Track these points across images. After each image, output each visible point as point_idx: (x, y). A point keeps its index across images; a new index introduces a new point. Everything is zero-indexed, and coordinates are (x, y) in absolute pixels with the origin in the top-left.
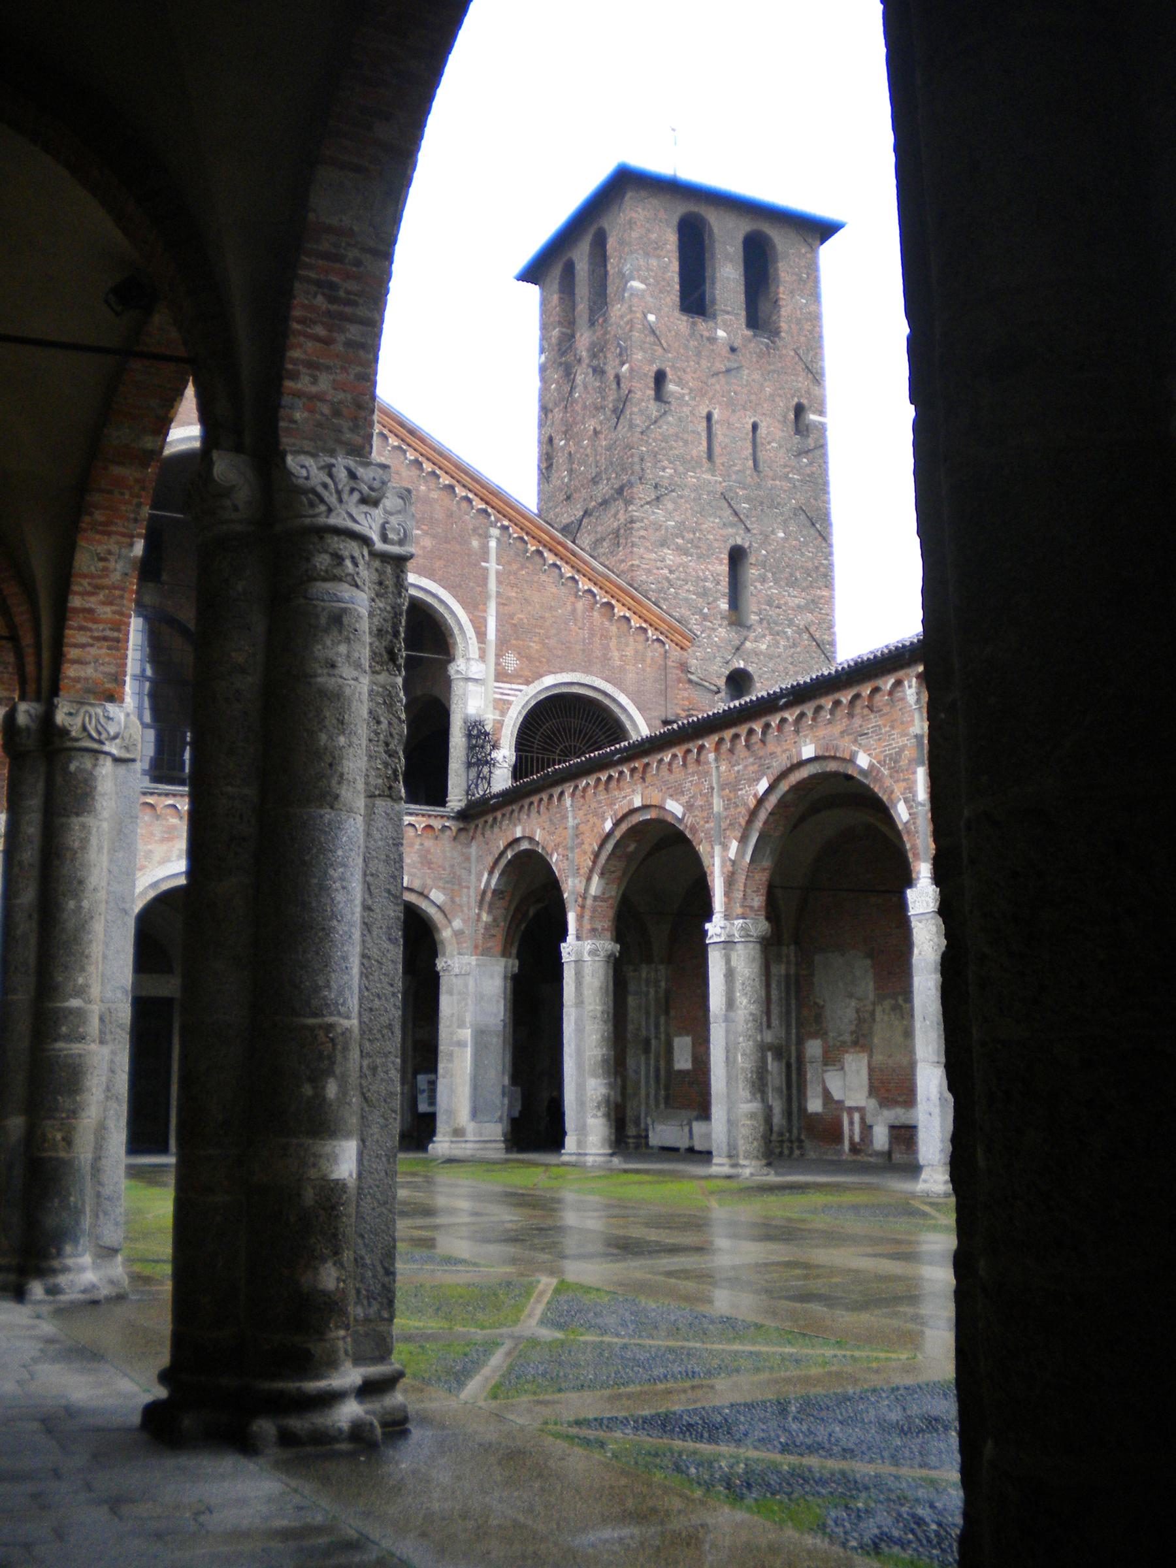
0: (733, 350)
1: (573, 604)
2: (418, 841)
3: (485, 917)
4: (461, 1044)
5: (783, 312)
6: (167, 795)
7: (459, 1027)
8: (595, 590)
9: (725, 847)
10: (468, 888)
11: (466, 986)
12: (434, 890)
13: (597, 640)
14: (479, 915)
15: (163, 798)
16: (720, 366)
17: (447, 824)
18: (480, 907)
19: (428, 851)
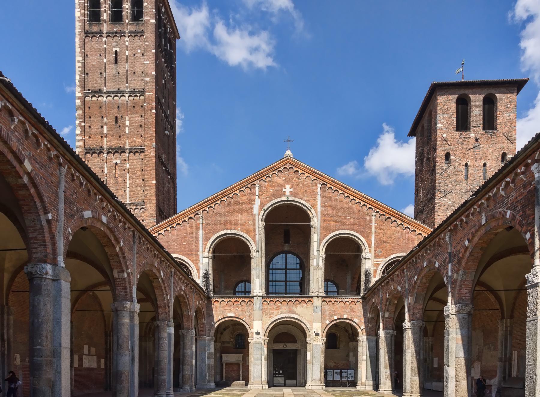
0: (477, 140)
1: (402, 232)
5: (498, 121)
6: (277, 298)
8: (409, 227)
9: (408, 299)
13: (410, 242)
16: (471, 146)
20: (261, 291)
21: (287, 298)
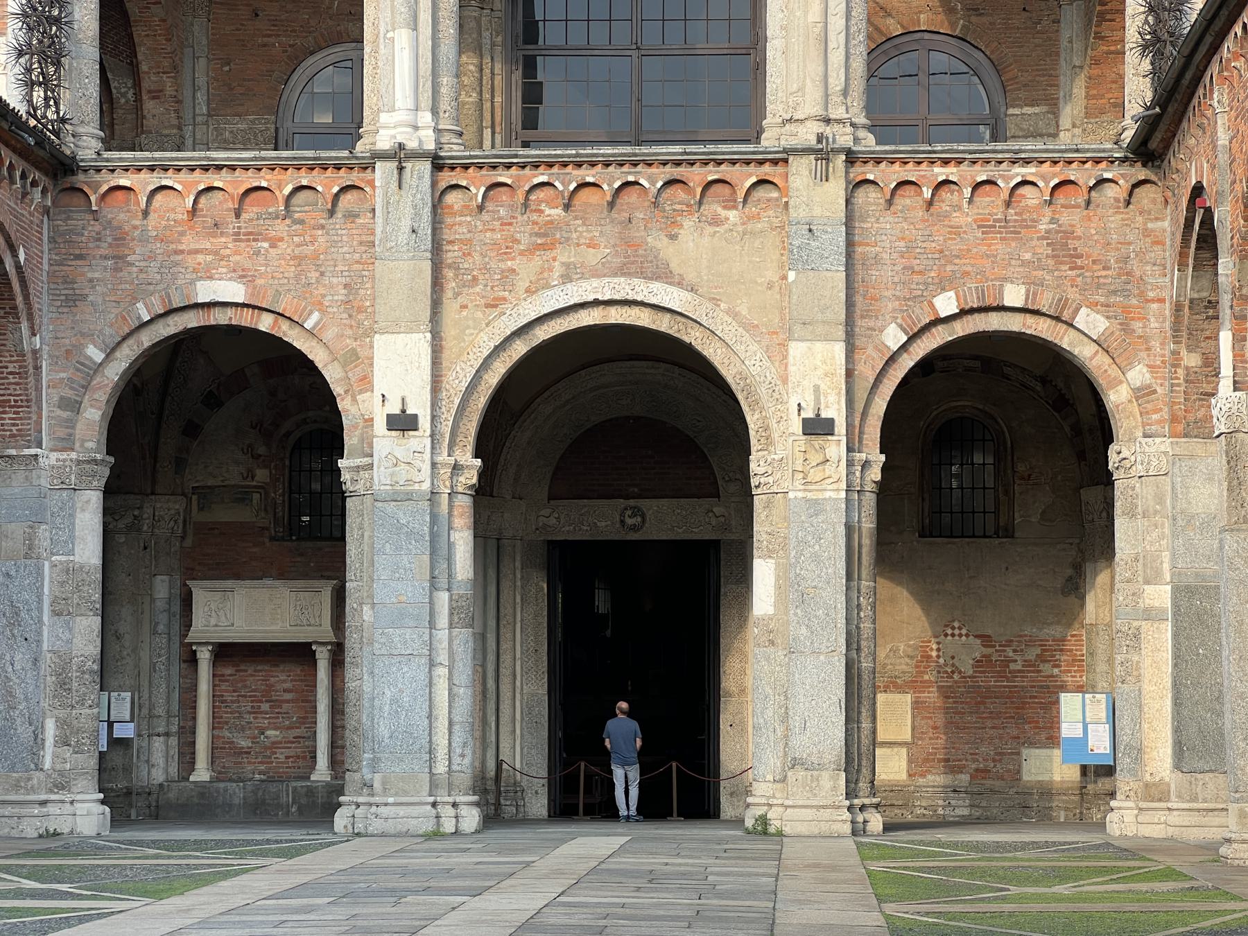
2: (1048, 211)
3: (1192, 360)
4: (1150, 615)
7: (1147, 582)
10: (1162, 301)
11: (1160, 499)
12: (1084, 311)
14: (1175, 353)
15: (527, 171)
17: (1107, 175)
18: (1176, 339)
19: (1069, 234)
20: (426, 118)
21: (607, 165)
